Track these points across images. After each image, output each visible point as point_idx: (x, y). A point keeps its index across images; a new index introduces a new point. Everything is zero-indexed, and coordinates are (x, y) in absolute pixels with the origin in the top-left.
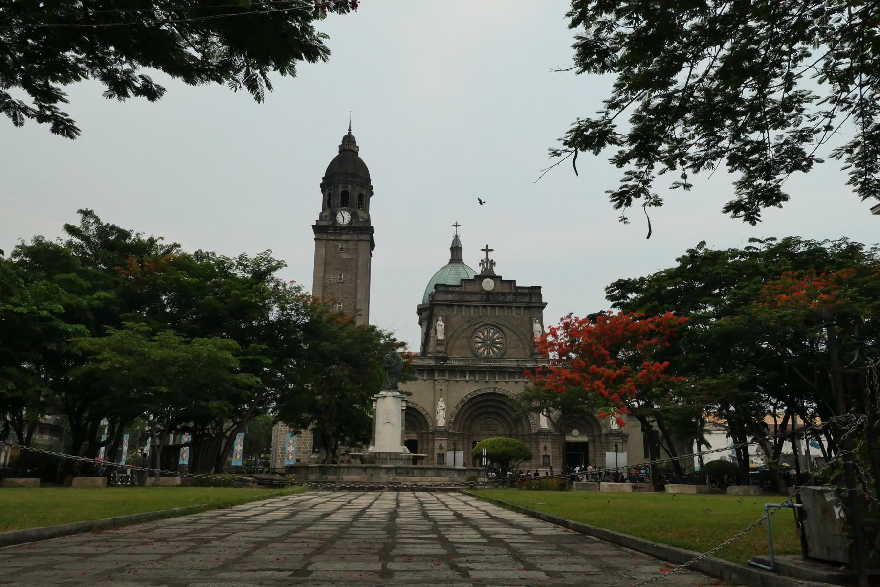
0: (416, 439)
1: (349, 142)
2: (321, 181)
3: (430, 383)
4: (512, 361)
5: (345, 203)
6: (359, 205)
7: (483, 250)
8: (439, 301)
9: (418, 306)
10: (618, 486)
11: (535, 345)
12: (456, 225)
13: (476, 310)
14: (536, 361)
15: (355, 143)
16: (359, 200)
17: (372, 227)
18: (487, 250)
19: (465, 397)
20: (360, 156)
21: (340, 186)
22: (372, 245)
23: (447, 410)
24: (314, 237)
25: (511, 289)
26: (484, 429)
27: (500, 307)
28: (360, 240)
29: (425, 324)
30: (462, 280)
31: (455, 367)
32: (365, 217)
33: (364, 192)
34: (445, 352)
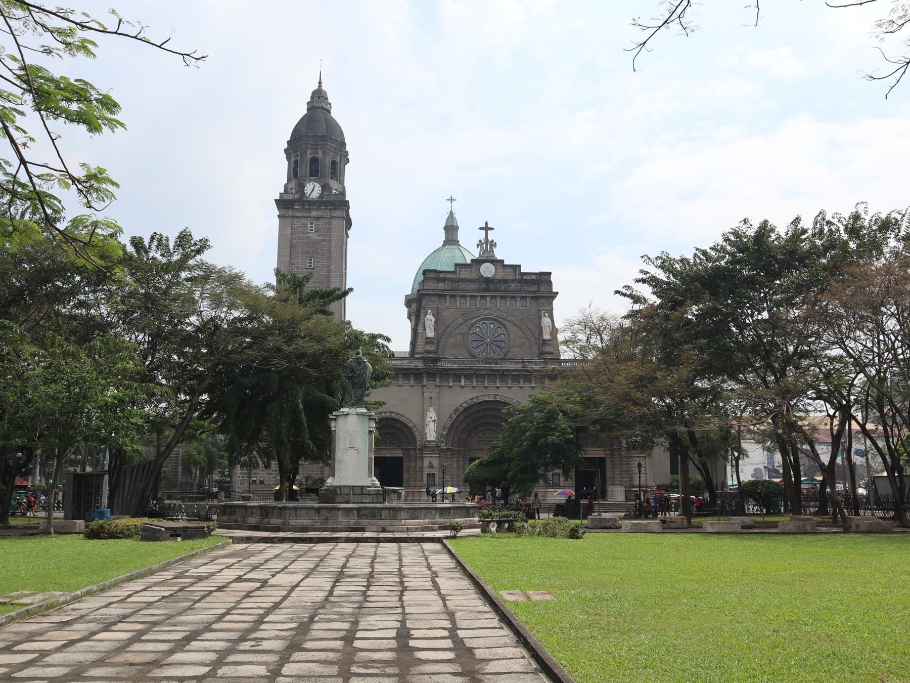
0: (401, 455)
1: (319, 98)
2: (286, 146)
3: (417, 389)
4: (516, 362)
5: (315, 172)
6: (332, 174)
7: (481, 229)
8: (428, 290)
9: (406, 296)
10: (644, 525)
11: (545, 342)
12: (451, 200)
13: (473, 301)
14: (546, 363)
15: (326, 99)
16: (332, 168)
17: (348, 202)
18: (486, 229)
19: (460, 406)
20: (332, 115)
21: (309, 152)
22: (349, 224)
23: (438, 421)
24: (278, 213)
25: (516, 275)
26: (482, 443)
27: (502, 297)
28: (335, 217)
29: (413, 318)
30: (456, 265)
31: (447, 370)
32: (340, 189)
33: (338, 160)
34: (436, 352)
